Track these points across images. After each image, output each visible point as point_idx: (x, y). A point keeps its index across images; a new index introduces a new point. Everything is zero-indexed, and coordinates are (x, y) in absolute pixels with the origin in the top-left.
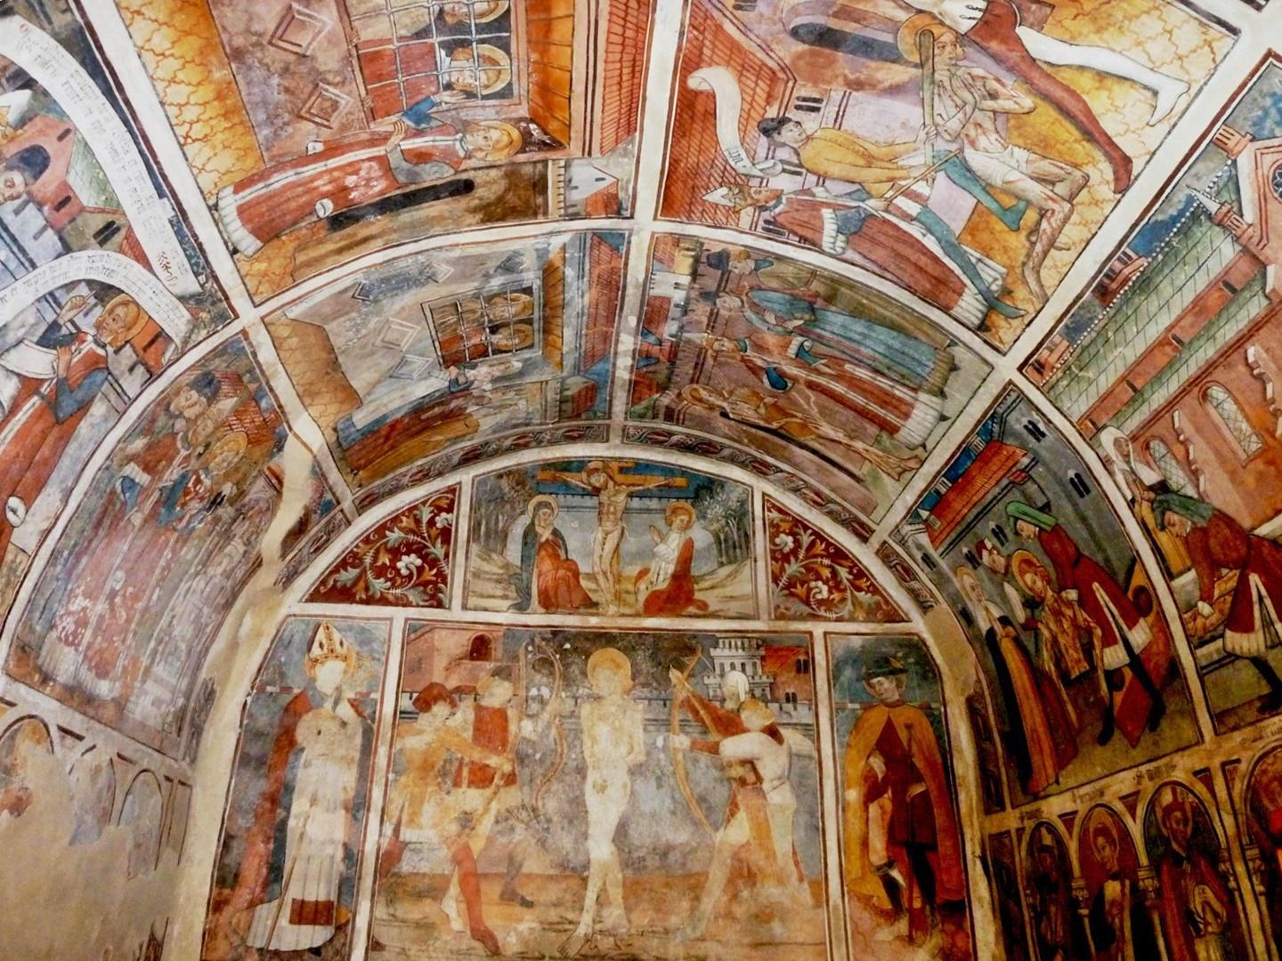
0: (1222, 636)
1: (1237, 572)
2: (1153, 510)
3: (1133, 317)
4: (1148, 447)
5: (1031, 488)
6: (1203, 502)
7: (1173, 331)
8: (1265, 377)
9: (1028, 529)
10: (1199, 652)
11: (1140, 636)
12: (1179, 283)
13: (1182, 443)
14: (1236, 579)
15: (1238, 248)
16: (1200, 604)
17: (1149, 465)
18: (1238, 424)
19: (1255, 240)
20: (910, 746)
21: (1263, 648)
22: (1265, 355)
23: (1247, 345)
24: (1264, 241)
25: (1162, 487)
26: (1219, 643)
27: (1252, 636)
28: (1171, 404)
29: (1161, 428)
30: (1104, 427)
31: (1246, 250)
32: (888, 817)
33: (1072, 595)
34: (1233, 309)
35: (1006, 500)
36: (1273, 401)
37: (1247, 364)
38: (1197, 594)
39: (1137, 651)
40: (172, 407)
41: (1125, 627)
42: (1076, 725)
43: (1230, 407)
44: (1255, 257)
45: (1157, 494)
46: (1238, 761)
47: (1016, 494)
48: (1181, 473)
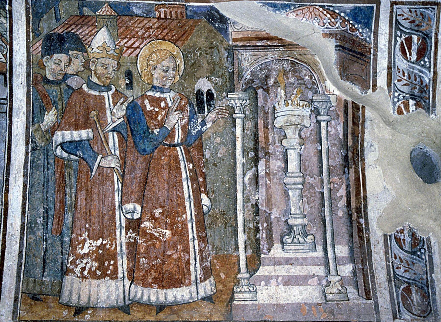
40: (50, 78)
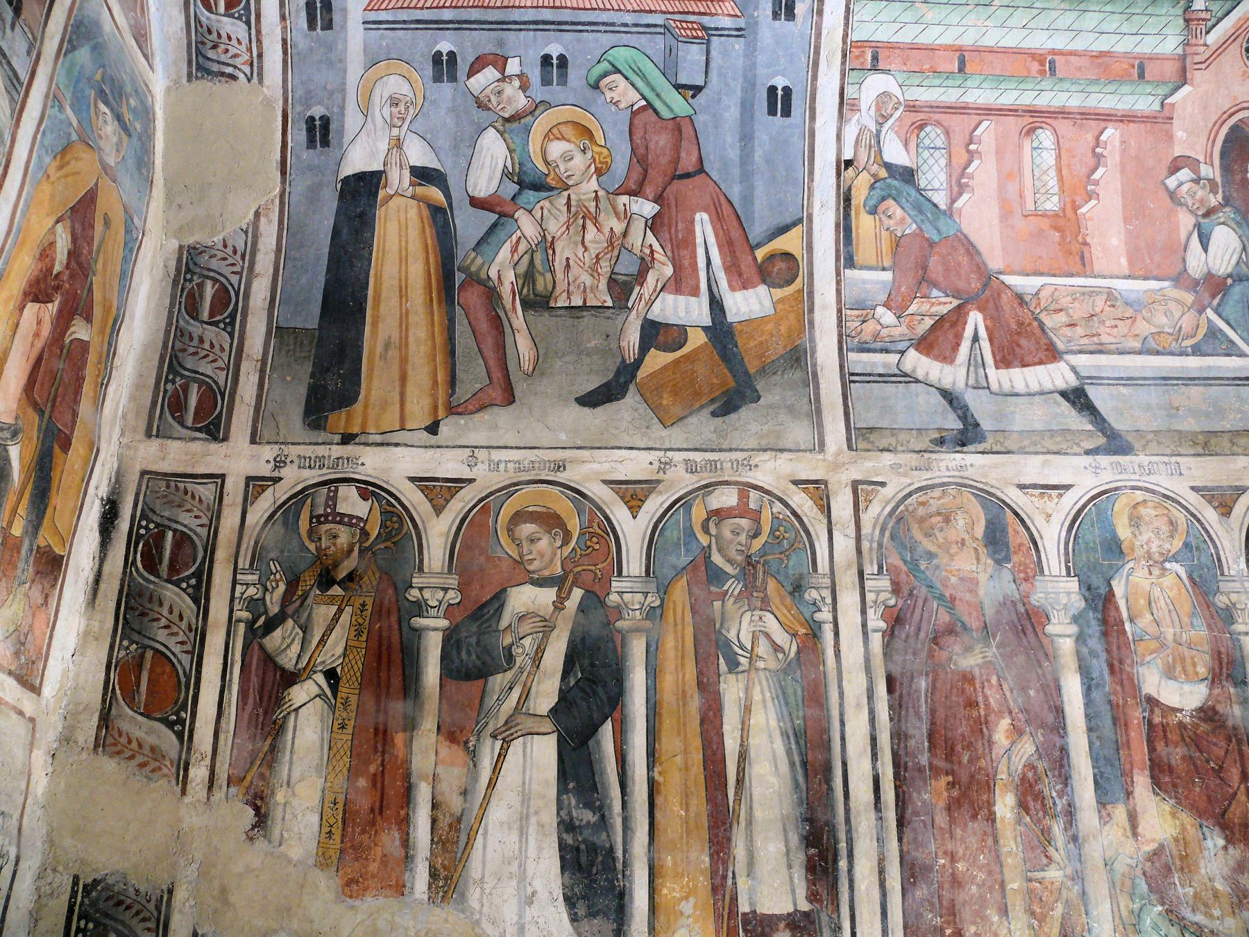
0: (903, 353)
1: (956, 303)
2: (872, 187)
3: (1035, 12)
4: (921, 127)
5: (694, 54)
6: (951, 216)
7: (1056, 58)
8: (1102, 160)
9: (623, 93)
10: (853, 356)
11: (748, 304)
12: (1105, 27)
13: (968, 151)
14: (949, 307)
15: (1180, 51)
16: (880, 310)
17: (906, 144)
18: (1045, 177)
19: (1198, 59)
20: (98, 252)
21: (961, 384)
22: (1117, 144)
23: (1111, 124)
24: (1203, 66)
25: (908, 175)
26: (893, 358)
27: (948, 368)
28: (988, 111)
29: (958, 123)
30: (887, 72)
31: (1183, 58)
32: (39, 344)
33: (647, 208)
34: (1126, 89)
35: (625, 38)
36: (1097, 183)
37: (1097, 139)
38: (883, 297)
39: (731, 318)
41: (723, 283)
42: (527, 365)
43: (1049, 158)
44: (1184, 69)
45: (892, 176)
46: (883, 484)
47: (658, 44)
48: (943, 177)
